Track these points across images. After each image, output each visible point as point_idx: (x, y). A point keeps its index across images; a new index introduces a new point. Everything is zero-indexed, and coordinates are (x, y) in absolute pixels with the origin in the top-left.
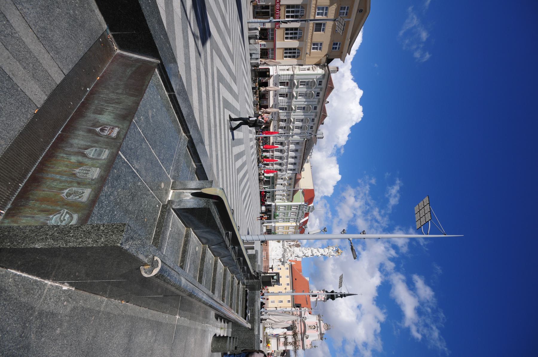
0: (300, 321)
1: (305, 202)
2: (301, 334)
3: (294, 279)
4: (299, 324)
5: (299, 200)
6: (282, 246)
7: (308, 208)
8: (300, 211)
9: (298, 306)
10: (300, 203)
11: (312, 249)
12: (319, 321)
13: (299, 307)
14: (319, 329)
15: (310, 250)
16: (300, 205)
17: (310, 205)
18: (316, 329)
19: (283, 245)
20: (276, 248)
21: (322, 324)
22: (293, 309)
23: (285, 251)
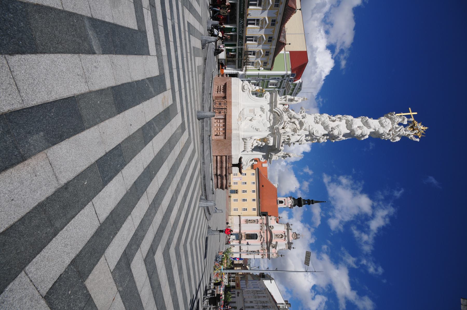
0: (266, 230)
1: (292, 70)
2: (267, 243)
3: (261, 186)
4: (265, 233)
5: (282, 68)
6: (267, 108)
7: (292, 87)
8: (281, 90)
9: (265, 214)
10: (283, 73)
11: (350, 118)
12: (288, 230)
13: (264, 215)
14: (287, 238)
15: (344, 121)
16: (283, 76)
17: (297, 82)
18: (284, 238)
19: (272, 104)
20: (253, 111)
21: (291, 233)
22: (259, 218)
23: (277, 117)
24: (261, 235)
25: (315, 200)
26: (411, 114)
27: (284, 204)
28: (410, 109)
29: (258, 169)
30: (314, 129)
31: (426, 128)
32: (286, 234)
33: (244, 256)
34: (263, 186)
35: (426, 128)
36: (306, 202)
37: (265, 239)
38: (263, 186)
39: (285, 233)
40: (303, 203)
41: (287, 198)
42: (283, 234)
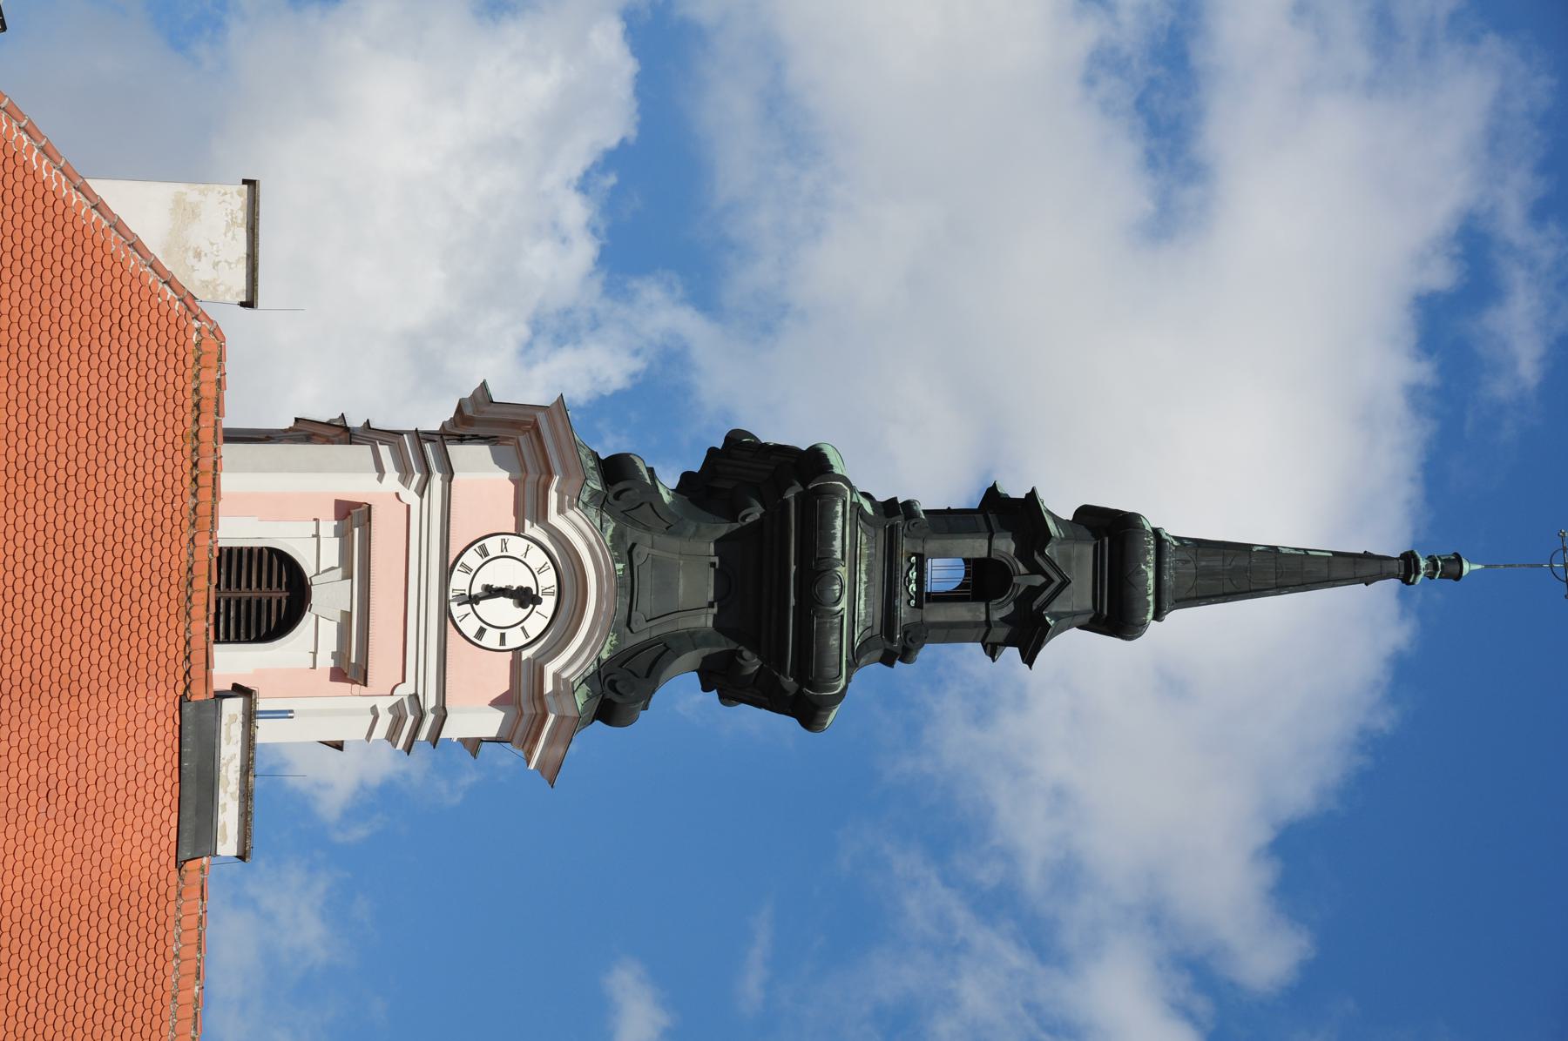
25: (1179, 510)
27: (314, 638)
40: (852, 599)
41: (424, 453)
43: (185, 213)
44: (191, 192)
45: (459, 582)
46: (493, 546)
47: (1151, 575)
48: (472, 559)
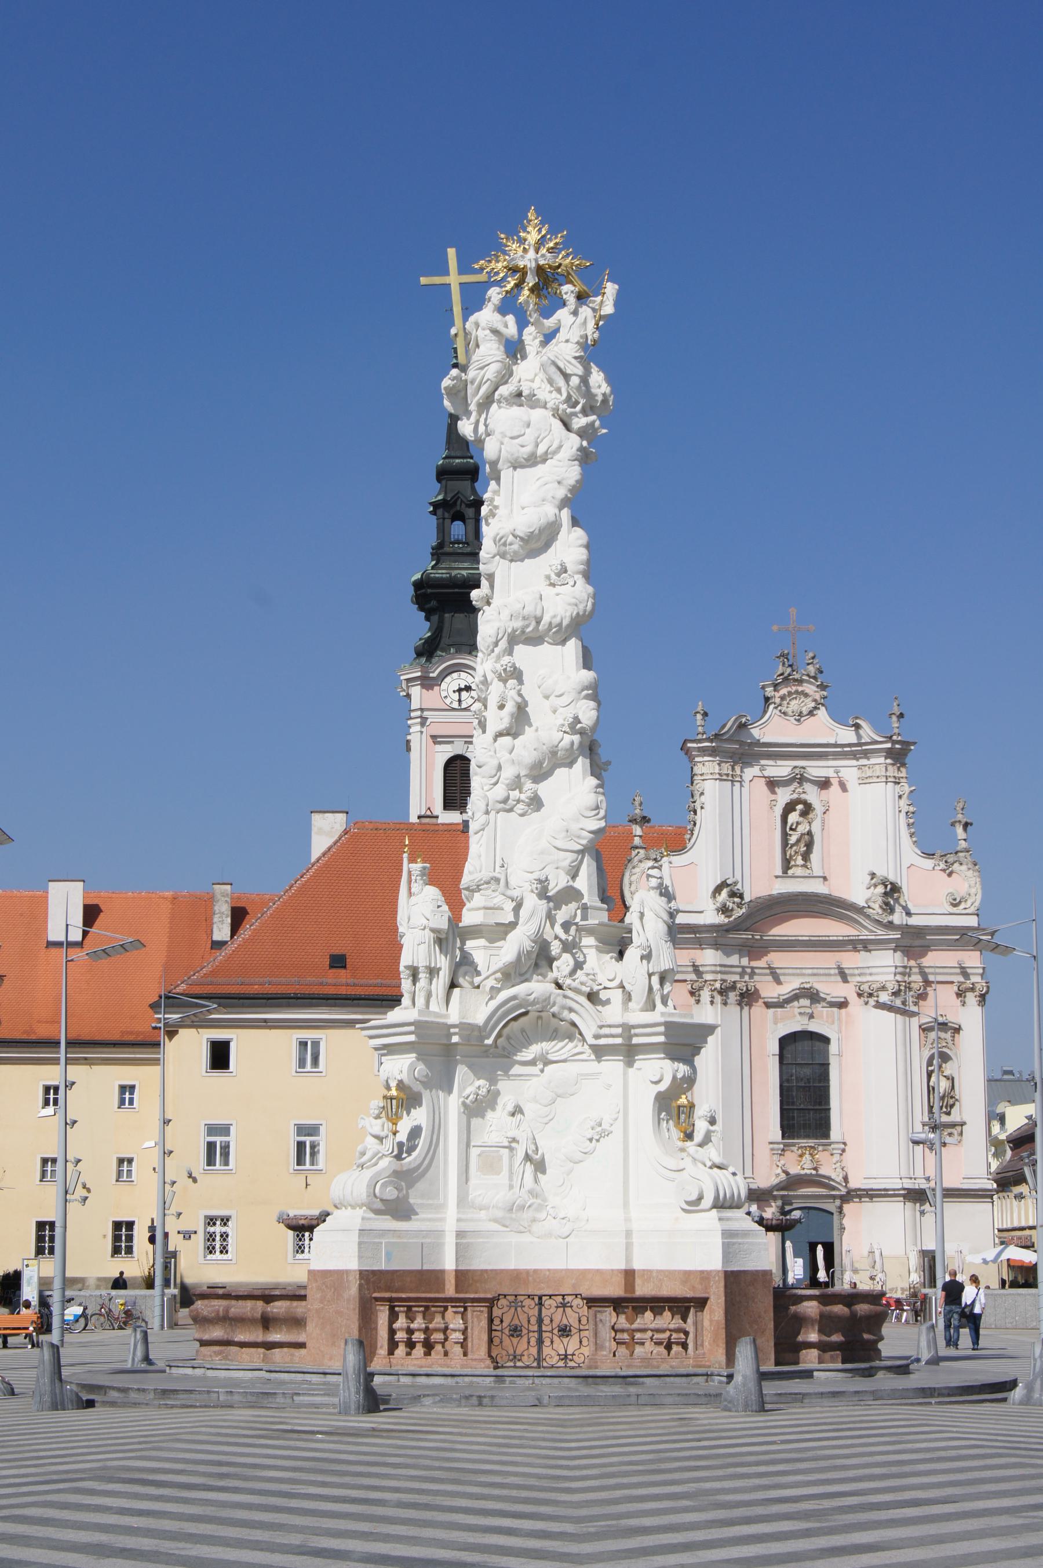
3: (340, 981)
18: (812, 794)
24: (796, 997)
26: (454, 279)
28: (423, 280)
29: (170, 1001)
30: (575, 827)
31: (531, 215)
32: (781, 769)
33: (972, 1160)
34: (338, 962)
35: (531, 215)
36: (457, 529)
37: (828, 960)
38: (338, 962)
39: (772, 784)
42: (784, 796)
43: (321, 831)
44: (314, 830)
45: (455, 705)
46: (444, 694)
47: (457, 461)
48: (448, 701)
